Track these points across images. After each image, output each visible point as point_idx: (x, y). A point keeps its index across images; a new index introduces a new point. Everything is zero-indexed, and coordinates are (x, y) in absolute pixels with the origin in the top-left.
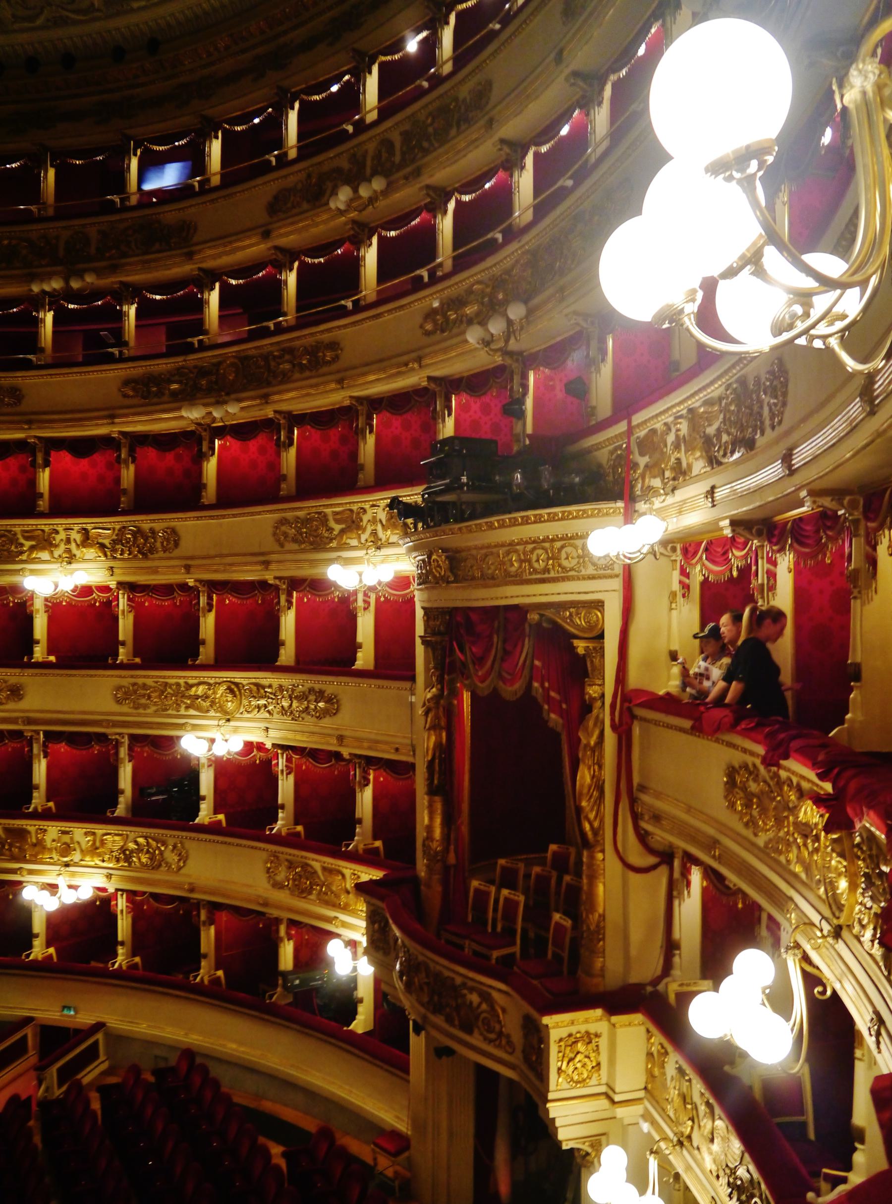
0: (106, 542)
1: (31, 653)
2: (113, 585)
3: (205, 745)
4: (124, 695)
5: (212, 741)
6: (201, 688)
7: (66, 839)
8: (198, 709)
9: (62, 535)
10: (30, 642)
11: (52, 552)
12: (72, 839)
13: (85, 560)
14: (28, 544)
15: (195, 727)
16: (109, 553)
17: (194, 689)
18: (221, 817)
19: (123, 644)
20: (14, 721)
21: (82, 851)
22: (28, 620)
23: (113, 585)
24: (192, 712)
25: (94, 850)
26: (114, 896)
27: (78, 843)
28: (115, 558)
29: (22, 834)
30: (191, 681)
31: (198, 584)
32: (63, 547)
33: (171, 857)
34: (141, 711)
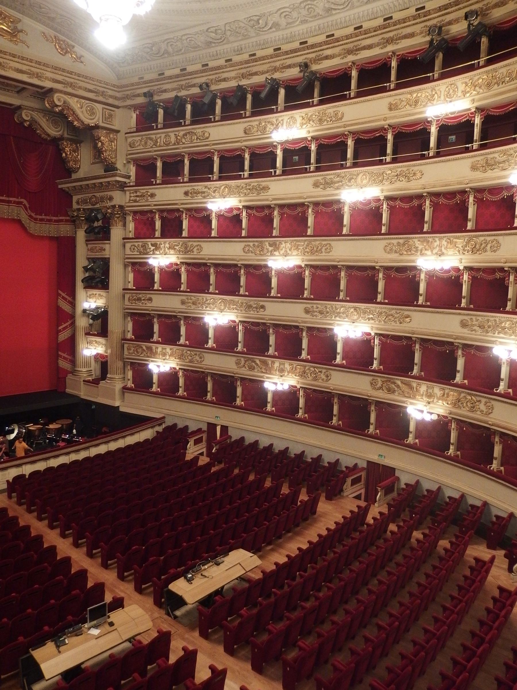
2: (461, 268)
3: (507, 353)
4: (464, 325)
5: (510, 351)
6: (508, 323)
8: (505, 333)
10: (417, 294)
11: (432, 251)
13: (448, 255)
15: (501, 343)
17: (504, 324)
18: (510, 391)
22: (417, 285)
23: (461, 268)
24: (502, 335)
26: (450, 421)
27: (436, 394)
28: (464, 254)
30: (503, 319)
31: (510, 269)
33: (482, 407)
34: (473, 332)
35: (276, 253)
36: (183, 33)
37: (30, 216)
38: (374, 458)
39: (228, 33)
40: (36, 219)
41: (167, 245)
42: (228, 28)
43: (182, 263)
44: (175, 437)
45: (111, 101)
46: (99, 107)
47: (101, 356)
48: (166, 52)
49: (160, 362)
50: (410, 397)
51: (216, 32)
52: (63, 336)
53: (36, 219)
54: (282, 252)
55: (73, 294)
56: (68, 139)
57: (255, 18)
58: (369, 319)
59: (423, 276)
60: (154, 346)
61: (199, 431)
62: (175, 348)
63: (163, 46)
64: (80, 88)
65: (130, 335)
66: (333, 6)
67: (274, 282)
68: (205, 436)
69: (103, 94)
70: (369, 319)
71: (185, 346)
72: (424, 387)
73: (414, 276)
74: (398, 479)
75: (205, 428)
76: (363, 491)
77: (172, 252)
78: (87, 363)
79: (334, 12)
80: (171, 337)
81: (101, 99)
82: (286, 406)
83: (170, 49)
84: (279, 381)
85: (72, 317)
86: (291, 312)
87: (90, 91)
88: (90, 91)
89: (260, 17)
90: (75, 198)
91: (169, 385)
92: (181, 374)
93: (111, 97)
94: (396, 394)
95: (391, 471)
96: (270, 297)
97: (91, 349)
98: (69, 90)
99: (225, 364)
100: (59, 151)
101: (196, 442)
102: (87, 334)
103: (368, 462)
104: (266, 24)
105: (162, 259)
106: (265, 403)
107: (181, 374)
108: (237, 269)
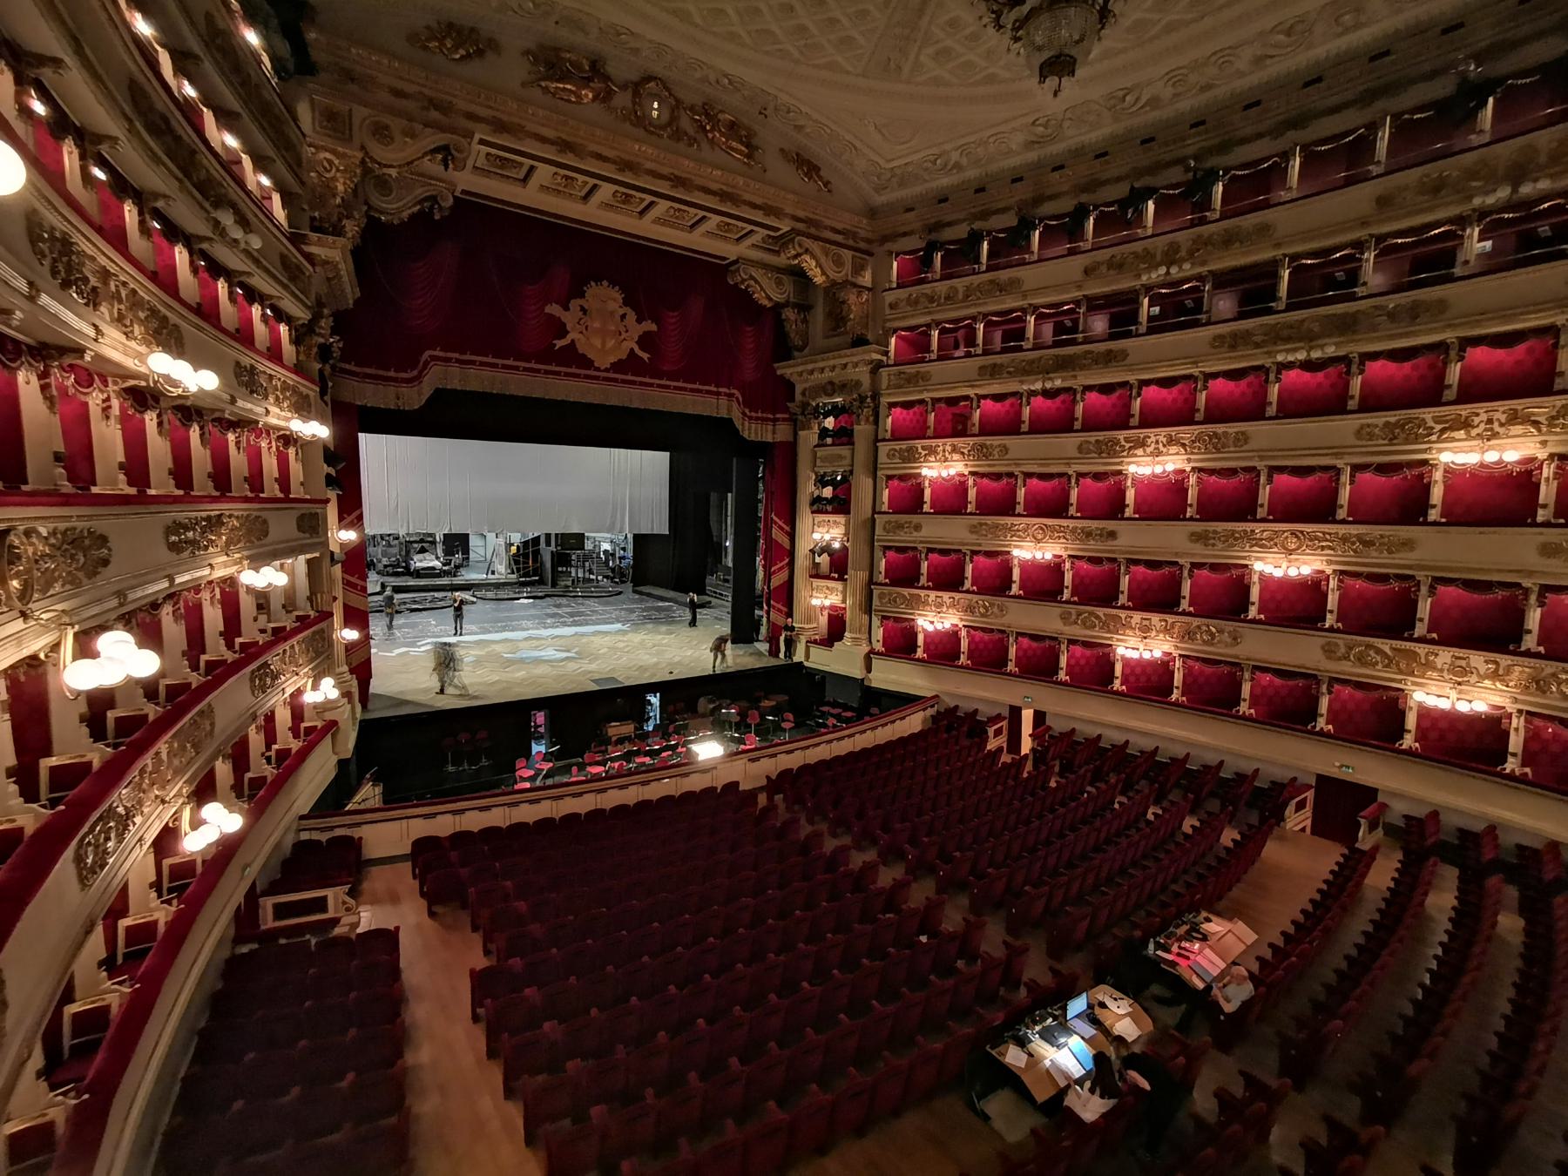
0: (1542, 419)
1: (1426, 515)
7: (1463, 663)
9: (1484, 417)
11: (1468, 433)
12: (1468, 664)
14: (1438, 427)
16: (1544, 429)
19: (1544, 506)
20: (1410, 567)
21: (1478, 674)
22: (1427, 489)
25: (1495, 676)
29: (1413, 655)
32: (1483, 426)
35: (1140, 452)
36: (993, 131)
37: (744, 414)
38: (1333, 772)
39: (1067, 124)
40: (750, 418)
41: (948, 448)
42: (1069, 115)
43: (972, 473)
44: (958, 727)
45: (862, 245)
46: (847, 255)
47: (832, 608)
48: (957, 166)
49: (931, 616)
50: (1412, 674)
51: (1046, 126)
52: (778, 579)
53: (750, 418)
54: (1149, 450)
55: (791, 520)
56: (795, 306)
57: (1121, 93)
58: (1323, 548)
59: (1438, 475)
60: (922, 593)
61: (998, 718)
62: (957, 596)
63: (955, 156)
64: (826, 228)
65: (881, 578)
66: (1272, 52)
67: (1130, 496)
68: (1004, 723)
69: (854, 236)
70: (1323, 548)
71: (973, 592)
72: (1445, 656)
73: (1421, 476)
74: (1384, 806)
75: (1006, 713)
76: (1309, 822)
77: (956, 456)
78: (810, 616)
79: (1268, 62)
80: (948, 580)
81: (851, 242)
82: (1150, 684)
83: (964, 161)
84: (1141, 644)
85: (791, 554)
86: (1170, 540)
87: (838, 232)
88: (838, 232)
89: (1129, 91)
90: (798, 389)
91: (943, 651)
92: (963, 633)
93: (863, 239)
94: (1379, 667)
95: (1366, 795)
96: (1123, 519)
97: (821, 598)
98: (813, 231)
99: (1045, 619)
100: (779, 323)
101: (998, 733)
102: (816, 573)
103: (1320, 777)
104: (1137, 99)
105: (942, 467)
106: (1111, 677)
107: (963, 633)
108: (1064, 479)
